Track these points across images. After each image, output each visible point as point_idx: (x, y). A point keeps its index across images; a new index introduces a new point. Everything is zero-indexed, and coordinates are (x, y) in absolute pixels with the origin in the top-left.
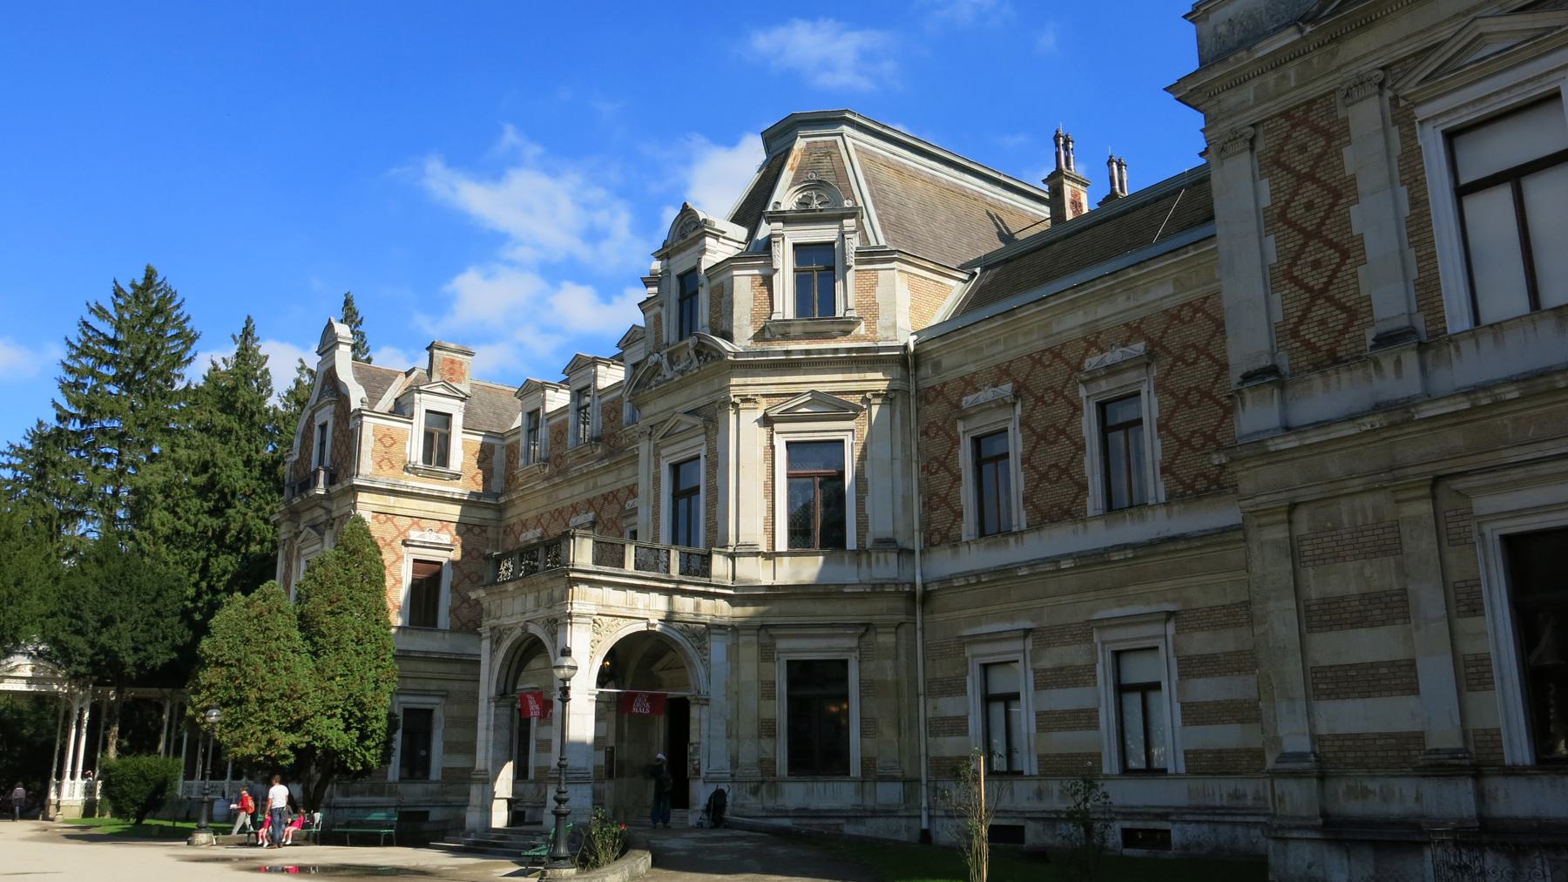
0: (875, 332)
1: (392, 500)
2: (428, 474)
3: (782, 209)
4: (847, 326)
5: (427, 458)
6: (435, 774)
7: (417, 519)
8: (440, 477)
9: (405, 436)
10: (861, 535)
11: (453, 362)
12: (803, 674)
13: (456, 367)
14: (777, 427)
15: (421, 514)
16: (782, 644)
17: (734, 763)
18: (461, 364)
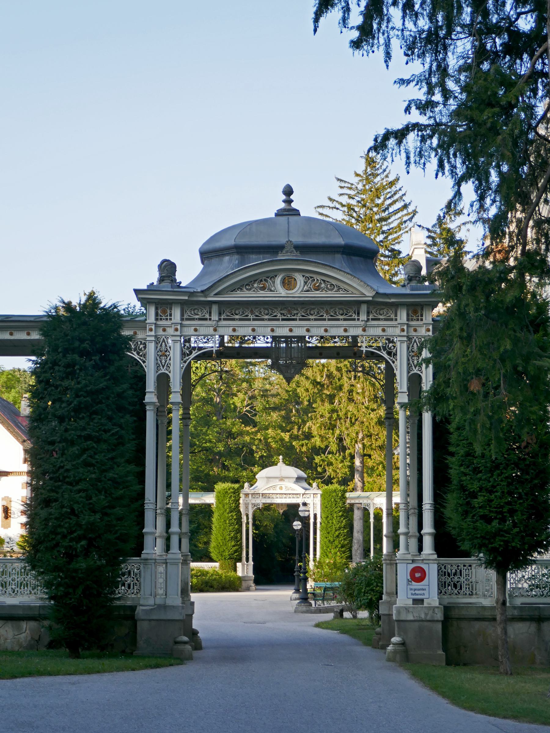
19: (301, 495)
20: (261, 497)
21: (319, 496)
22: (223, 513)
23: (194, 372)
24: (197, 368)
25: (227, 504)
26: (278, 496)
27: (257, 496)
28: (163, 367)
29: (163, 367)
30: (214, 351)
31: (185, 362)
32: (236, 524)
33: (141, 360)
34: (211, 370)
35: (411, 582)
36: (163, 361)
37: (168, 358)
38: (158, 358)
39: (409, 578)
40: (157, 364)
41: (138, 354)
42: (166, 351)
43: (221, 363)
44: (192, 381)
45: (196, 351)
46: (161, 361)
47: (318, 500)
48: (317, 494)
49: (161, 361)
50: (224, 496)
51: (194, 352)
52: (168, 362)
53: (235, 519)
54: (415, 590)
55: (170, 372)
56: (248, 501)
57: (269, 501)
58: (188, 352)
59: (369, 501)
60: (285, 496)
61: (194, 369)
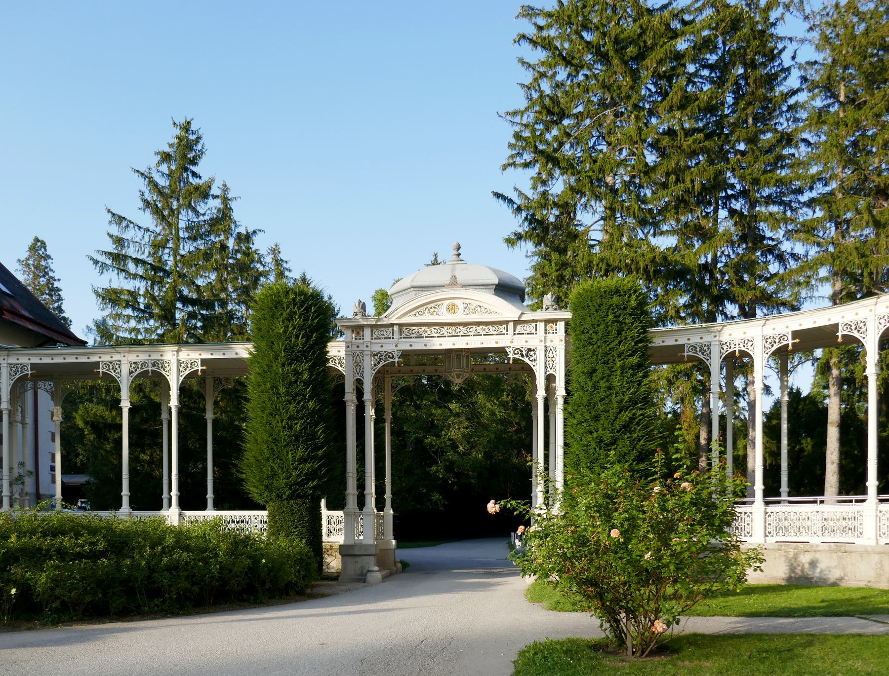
19: (511, 325)
20: (396, 336)
21: (561, 326)
22: (270, 366)
25: (279, 336)
26: (444, 330)
27: (387, 333)
32: (311, 398)
47: (558, 339)
48: (555, 321)
50: (273, 316)
53: (307, 383)
56: (362, 348)
57: (418, 345)
59: (707, 338)
60: (463, 330)
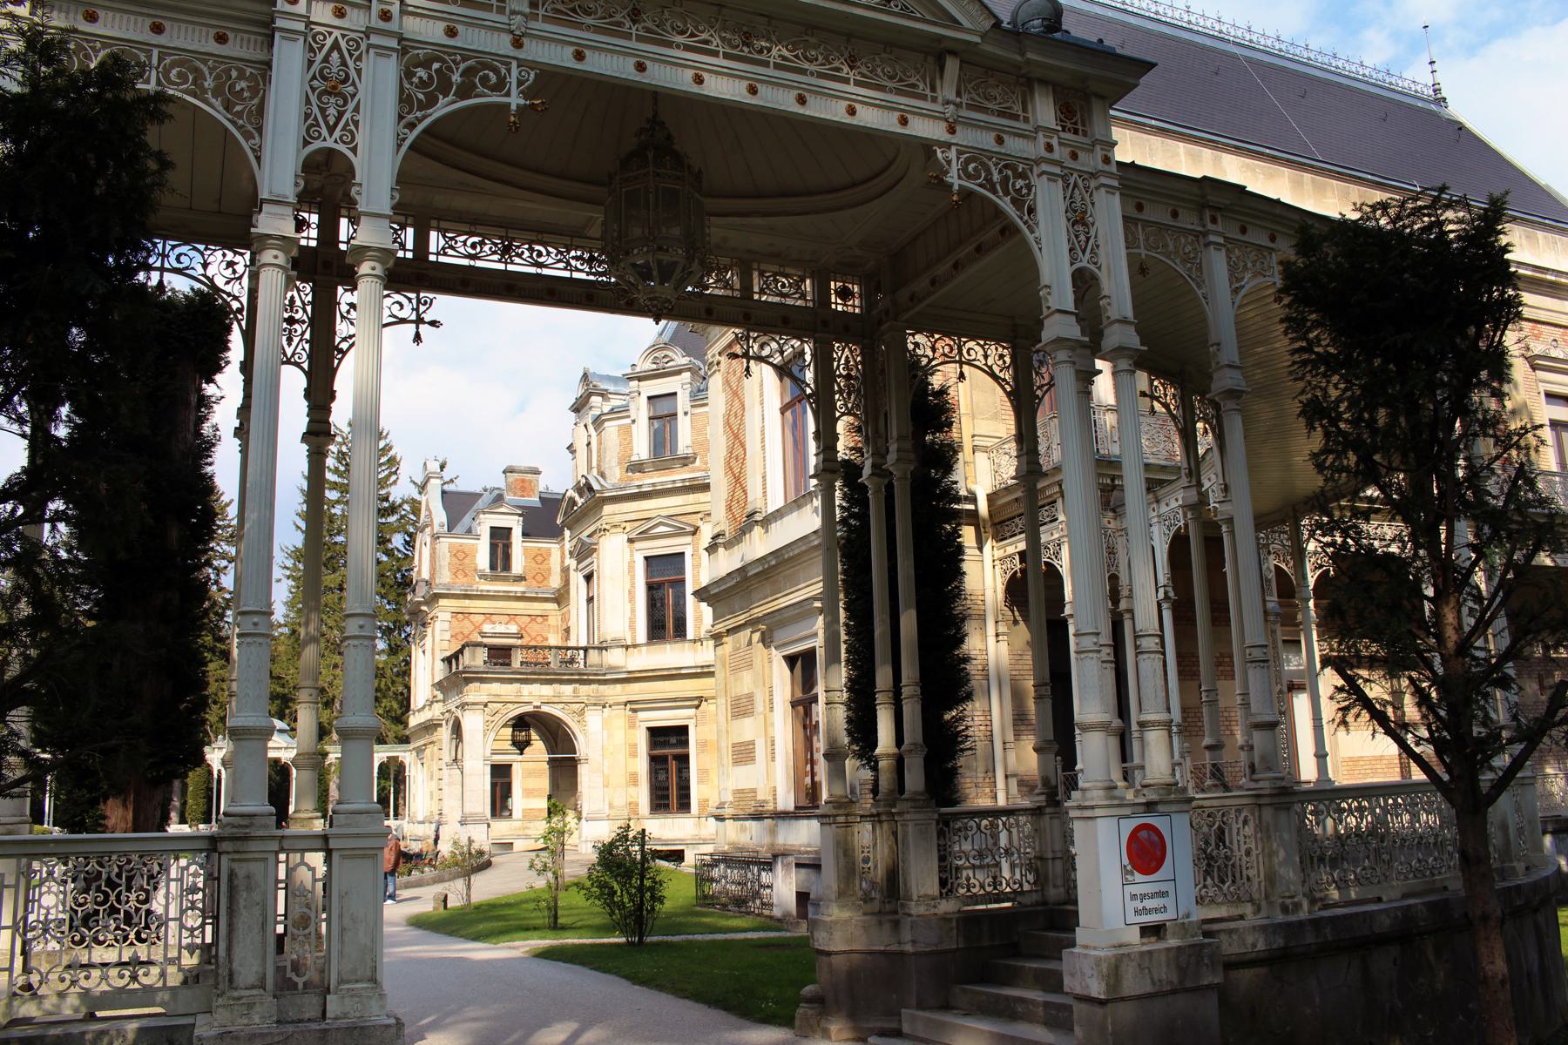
0: (706, 463)
1: (467, 602)
2: (495, 579)
3: (638, 369)
4: (686, 461)
5: (493, 567)
6: (517, 813)
7: (488, 616)
8: (505, 579)
9: (474, 550)
10: (698, 627)
11: (523, 481)
12: (658, 736)
13: (527, 485)
14: (638, 545)
15: (491, 611)
16: (641, 715)
17: (611, 806)
18: (530, 482)
23: (342, 317)
24: (353, 306)
28: (331, 130)
29: (331, 130)
30: (513, 107)
31: (411, 126)
33: (239, 128)
34: (395, 317)
35: (1132, 874)
36: (332, 111)
37: (351, 106)
38: (314, 99)
39: (1126, 861)
40: (307, 116)
41: (228, 107)
42: (344, 81)
43: (419, 301)
44: (338, 340)
45: (451, 97)
46: (323, 111)
49: (323, 111)
51: (442, 101)
52: (348, 115)
54: (1143, 897)
55: (354, 150)
58: (421, 96)
61: (344, 308)
